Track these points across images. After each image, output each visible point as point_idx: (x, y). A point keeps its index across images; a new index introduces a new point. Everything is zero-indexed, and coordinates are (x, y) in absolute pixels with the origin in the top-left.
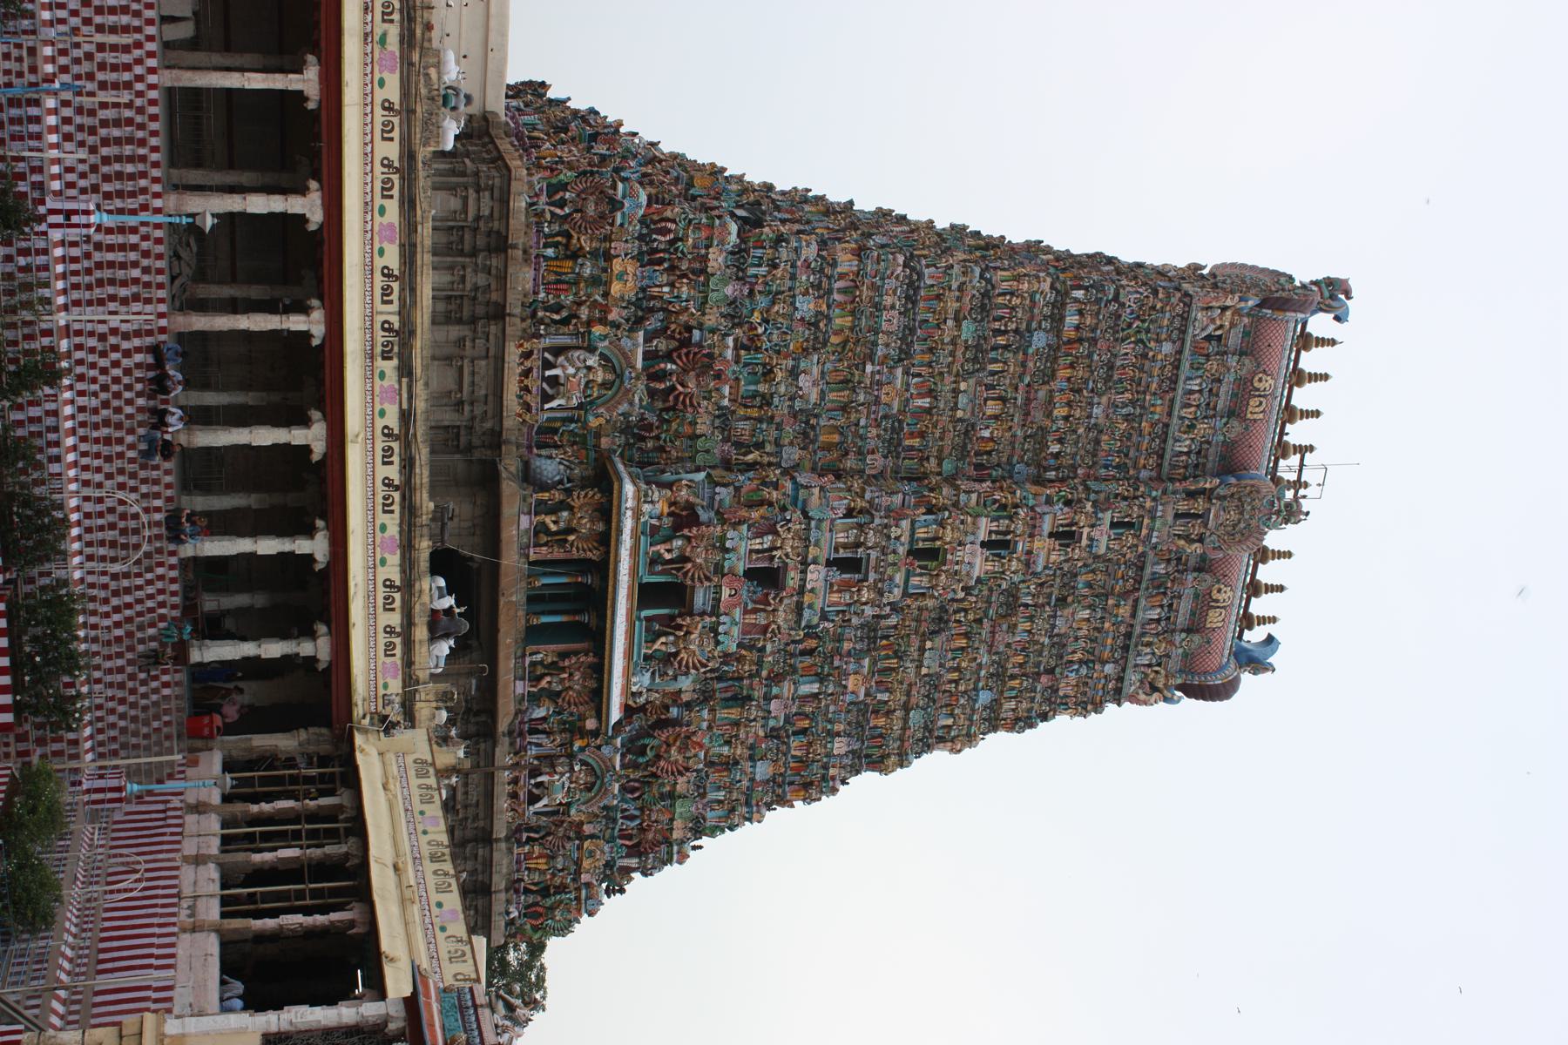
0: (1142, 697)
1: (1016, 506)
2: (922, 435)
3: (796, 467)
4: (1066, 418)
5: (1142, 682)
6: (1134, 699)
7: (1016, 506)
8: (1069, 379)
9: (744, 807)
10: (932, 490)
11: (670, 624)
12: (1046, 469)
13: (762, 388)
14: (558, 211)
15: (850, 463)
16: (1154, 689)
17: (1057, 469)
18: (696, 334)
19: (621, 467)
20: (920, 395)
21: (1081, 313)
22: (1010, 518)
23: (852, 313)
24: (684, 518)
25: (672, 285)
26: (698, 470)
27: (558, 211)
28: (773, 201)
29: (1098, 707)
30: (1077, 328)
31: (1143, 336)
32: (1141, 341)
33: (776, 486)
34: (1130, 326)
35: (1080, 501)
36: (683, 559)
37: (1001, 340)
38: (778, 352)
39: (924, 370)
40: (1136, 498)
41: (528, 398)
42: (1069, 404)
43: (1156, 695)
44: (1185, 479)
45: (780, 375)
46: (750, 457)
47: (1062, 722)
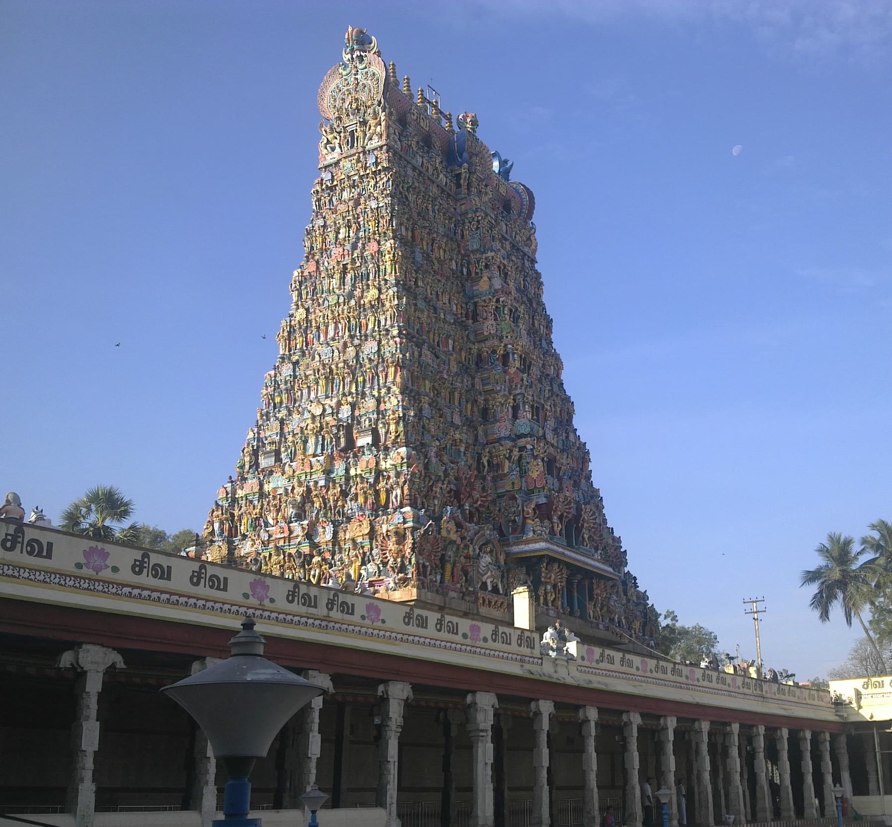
0: (533, 247)
1: (498, 301)
2: (461, 349)
3: (486, 434)
4: (445, 251)
5: (526, 245)
6: (535, 251)
7: (498, 301)
8: (428, 244)
9: (594, 498)
10: (494, 352)
11: (579, 530)
12: (462, 272)
13: (462, 449)
14: (429, 569)
15: (481, 399)
16: (529, 239)
17: (462, 266)
18: (453, 487)
19: (515, 549)
20: (447, 345)
21: (401, 224)
22: (504, 306)
23: (424, 379)
24: (544, 512)
25: (434, 497)
26: (514, 498)
27: (429, 569)
28: (323, 415)
29: (538, 275)
30: (407, 229)
31: (406, 186)
32: (408, 188)
33: (511, 451)
34: (401, 193)
35: (486, 258)
36: (561, 518)
37: (420, 283)
38: (447, 434)
39: (436, 341)
40: (478, 221)
41: (499, 603)
42: (439, 248)
43: (532, 239)
44: (459, 186)
45: (457, 436)
46: (486, 464)
47: (545, 299)
